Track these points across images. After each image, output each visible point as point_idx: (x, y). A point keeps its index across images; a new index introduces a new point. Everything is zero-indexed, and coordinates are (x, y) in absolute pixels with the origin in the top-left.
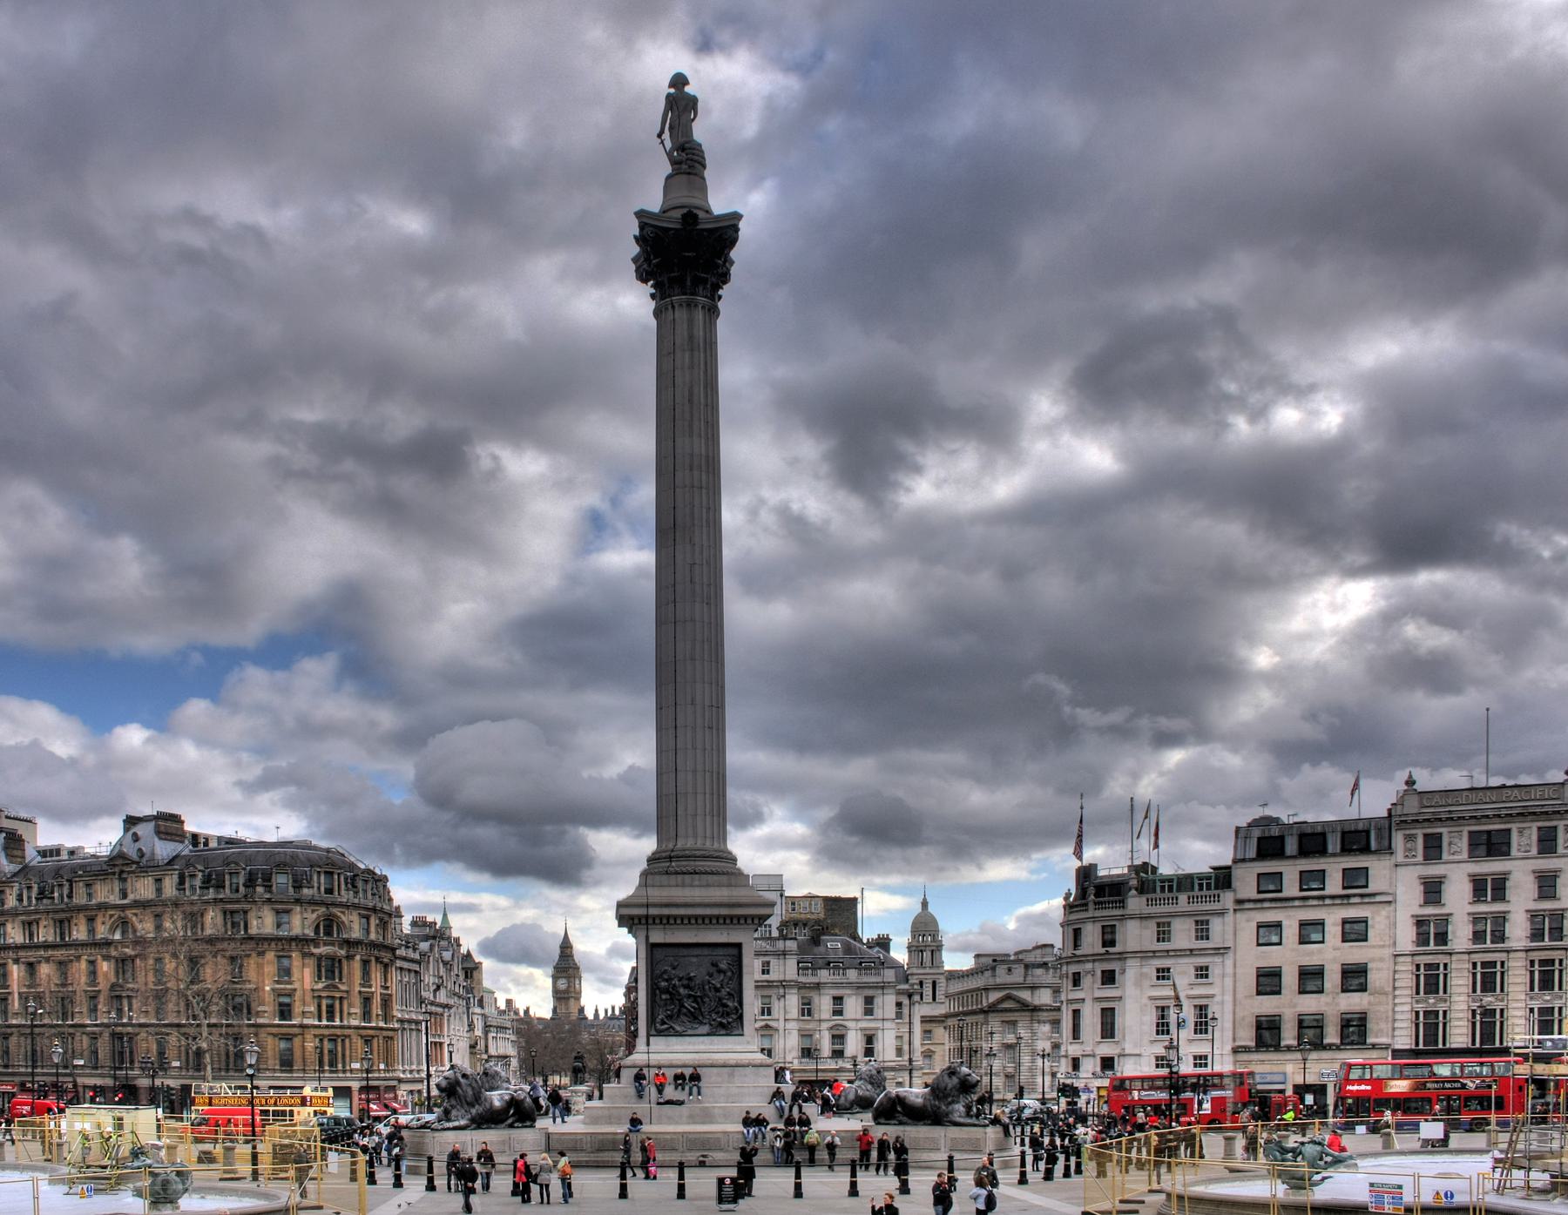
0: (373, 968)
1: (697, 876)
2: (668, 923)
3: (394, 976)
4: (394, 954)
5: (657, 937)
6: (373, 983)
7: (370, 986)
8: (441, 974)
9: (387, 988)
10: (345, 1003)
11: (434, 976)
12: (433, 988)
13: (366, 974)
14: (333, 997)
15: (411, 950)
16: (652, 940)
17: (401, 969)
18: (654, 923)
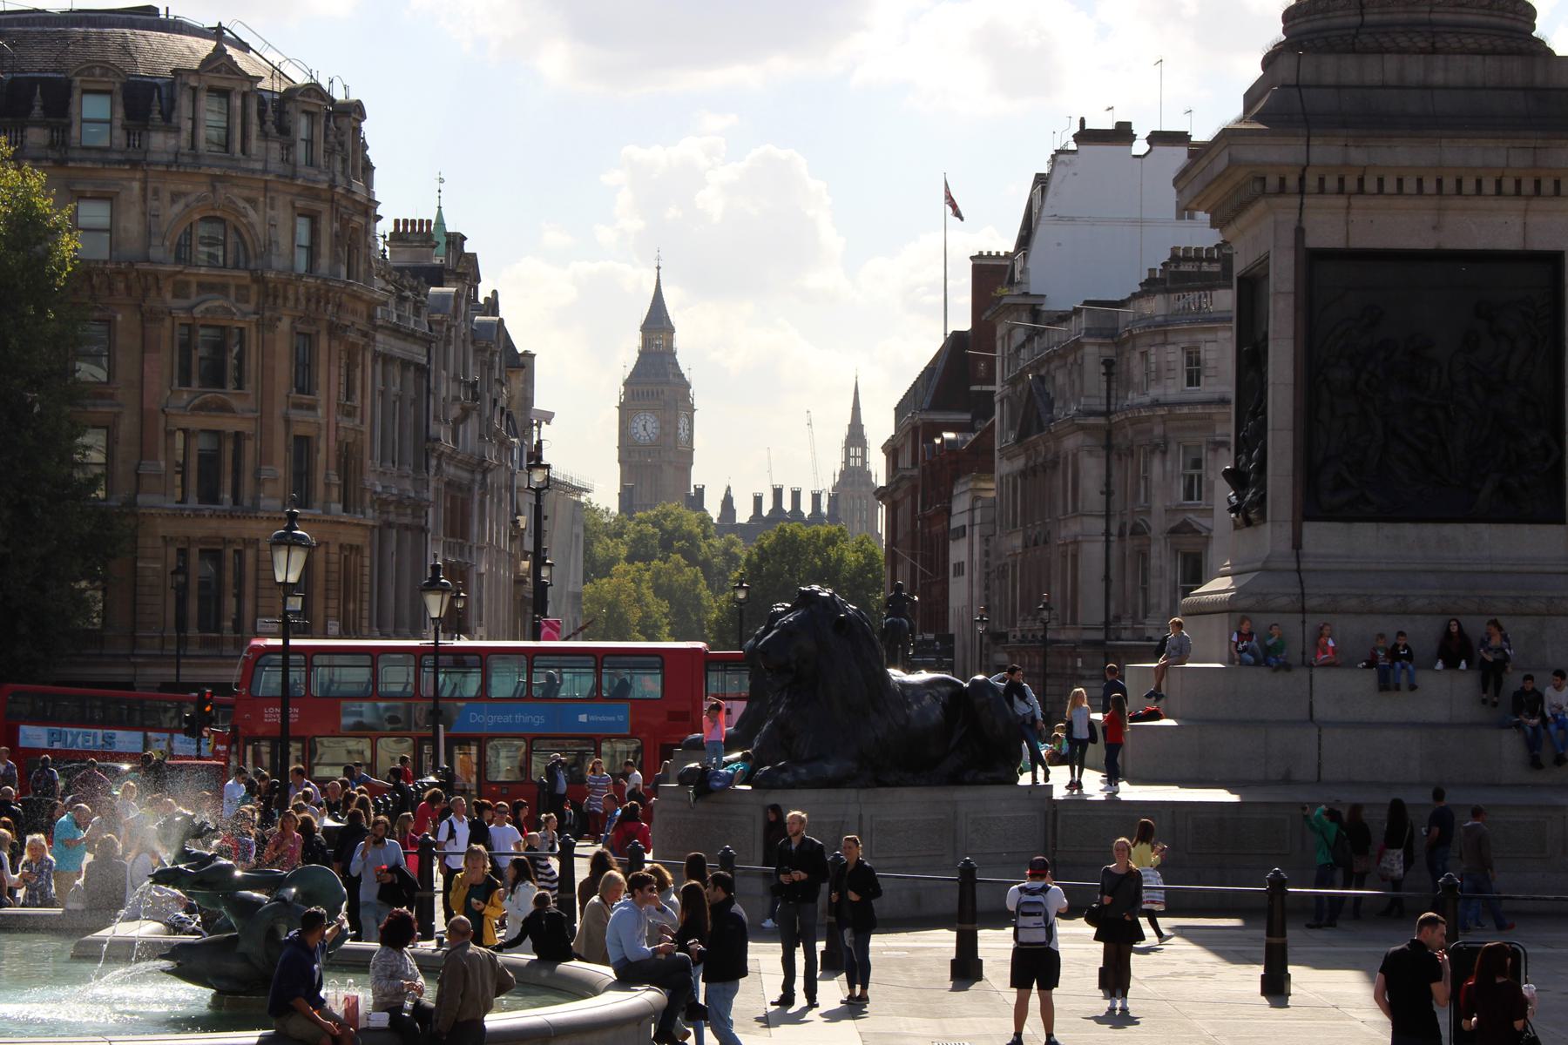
0: (323, 357)
1: (1439, 60)
2: (1361, 190)
3: (369, 375)
4: (371, 317)
5: (1327, 231)
6: (321, 396)
7: (312, 407)
8: (473, 376)
9: (350, 413)
10: (249, 448)
11: (456, 378)
12: (455, 411)
13: (304, 382)
14: (217, 434)
15: (408, 309)
16: (1314, 241)
17: (387, 359)
18: (1322, 190)
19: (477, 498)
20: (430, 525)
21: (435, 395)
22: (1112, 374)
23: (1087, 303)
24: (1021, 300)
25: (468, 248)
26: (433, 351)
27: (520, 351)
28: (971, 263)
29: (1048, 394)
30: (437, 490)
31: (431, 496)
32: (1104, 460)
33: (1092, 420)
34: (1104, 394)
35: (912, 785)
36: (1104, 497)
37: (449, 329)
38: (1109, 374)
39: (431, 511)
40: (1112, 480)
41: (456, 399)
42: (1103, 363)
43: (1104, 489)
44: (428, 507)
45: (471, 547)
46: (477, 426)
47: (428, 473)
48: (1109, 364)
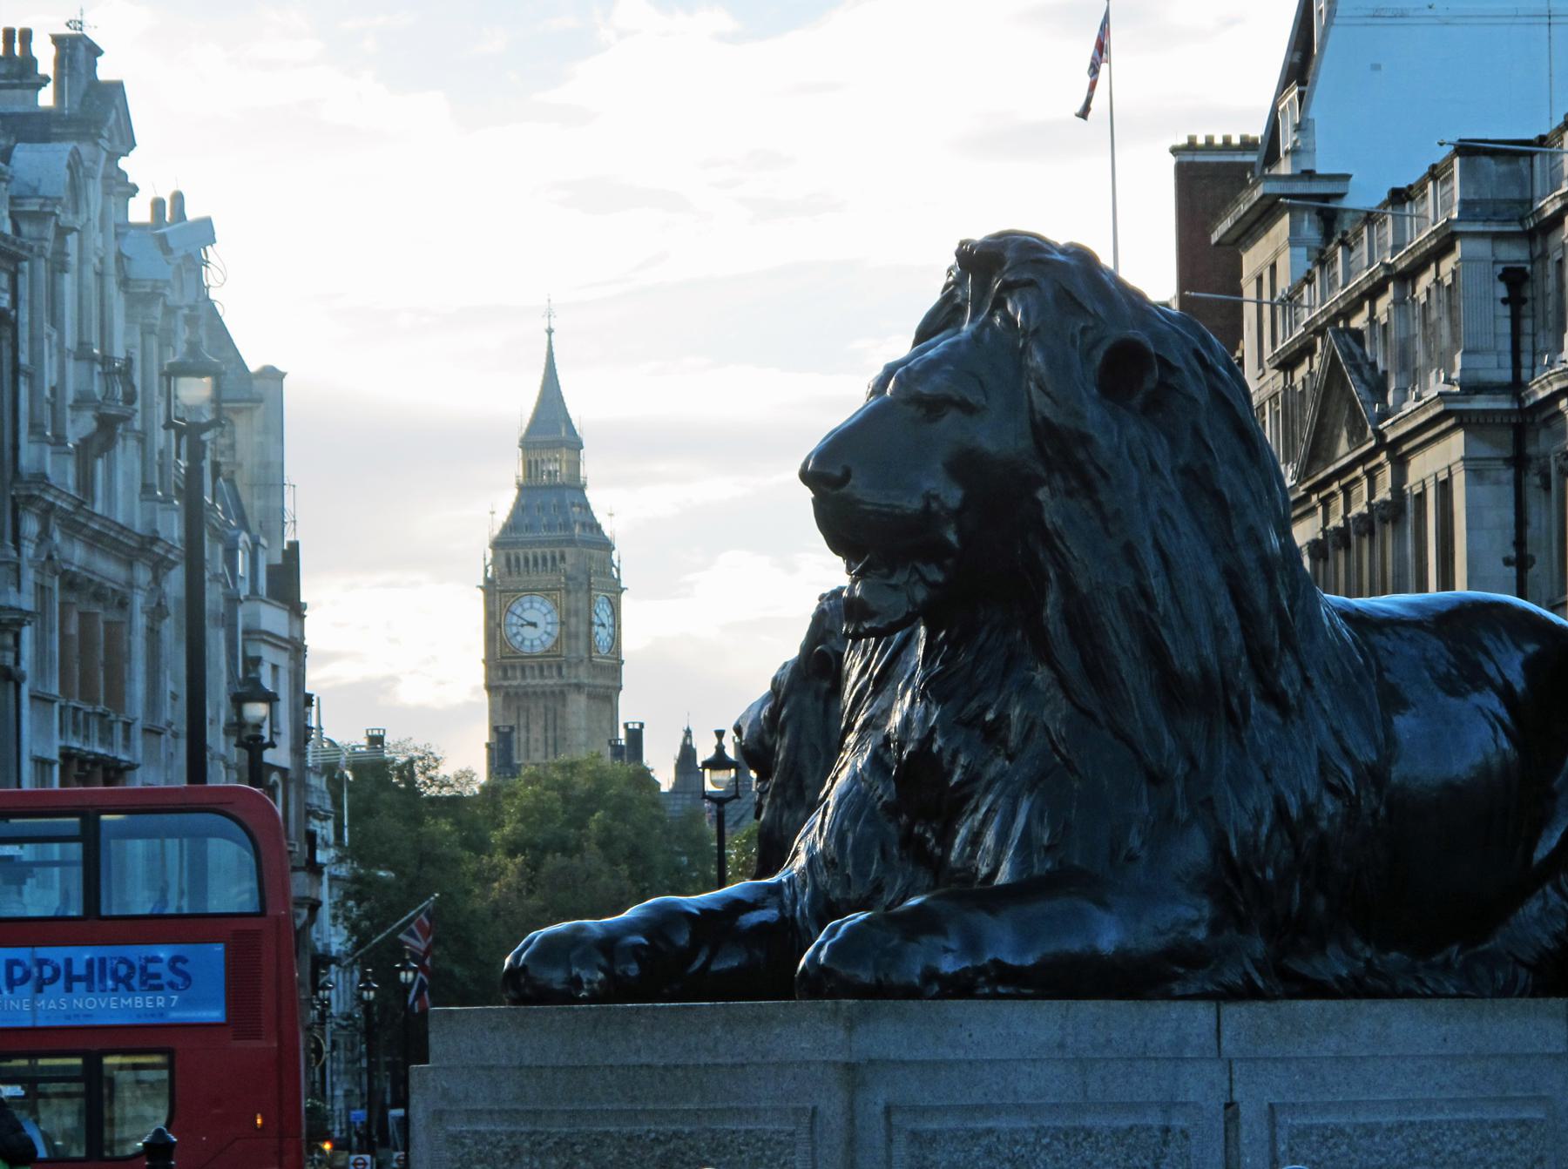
11: (83, 353)
19: (140, 621)
20: (26, 665)
21: (30, 376)
22: (1524, 301)
23: (1467, 150)
24: (1300, 188)
25: (105, 71)
26: (24, 282)
27: (253, 366)
28: (1171, 161)
29: (1373, 365)
30: (41, 589)
31: (27, 602)
32: (1509, 491)
33: (1480, 403)
34: (1506, 344)
35: (1408, 994)
36: (1512, 571)
37: (62, 232)
38: (1515, 301)
39: (27, 633)
40: (1530, 532)
41: (82, 401)
42: (1502, 277)
43: (1512, 553)
44: (20, 624)
45: (127, 726)
46: (137, 466)
47: (18, 548)
48: (1515, 279)
